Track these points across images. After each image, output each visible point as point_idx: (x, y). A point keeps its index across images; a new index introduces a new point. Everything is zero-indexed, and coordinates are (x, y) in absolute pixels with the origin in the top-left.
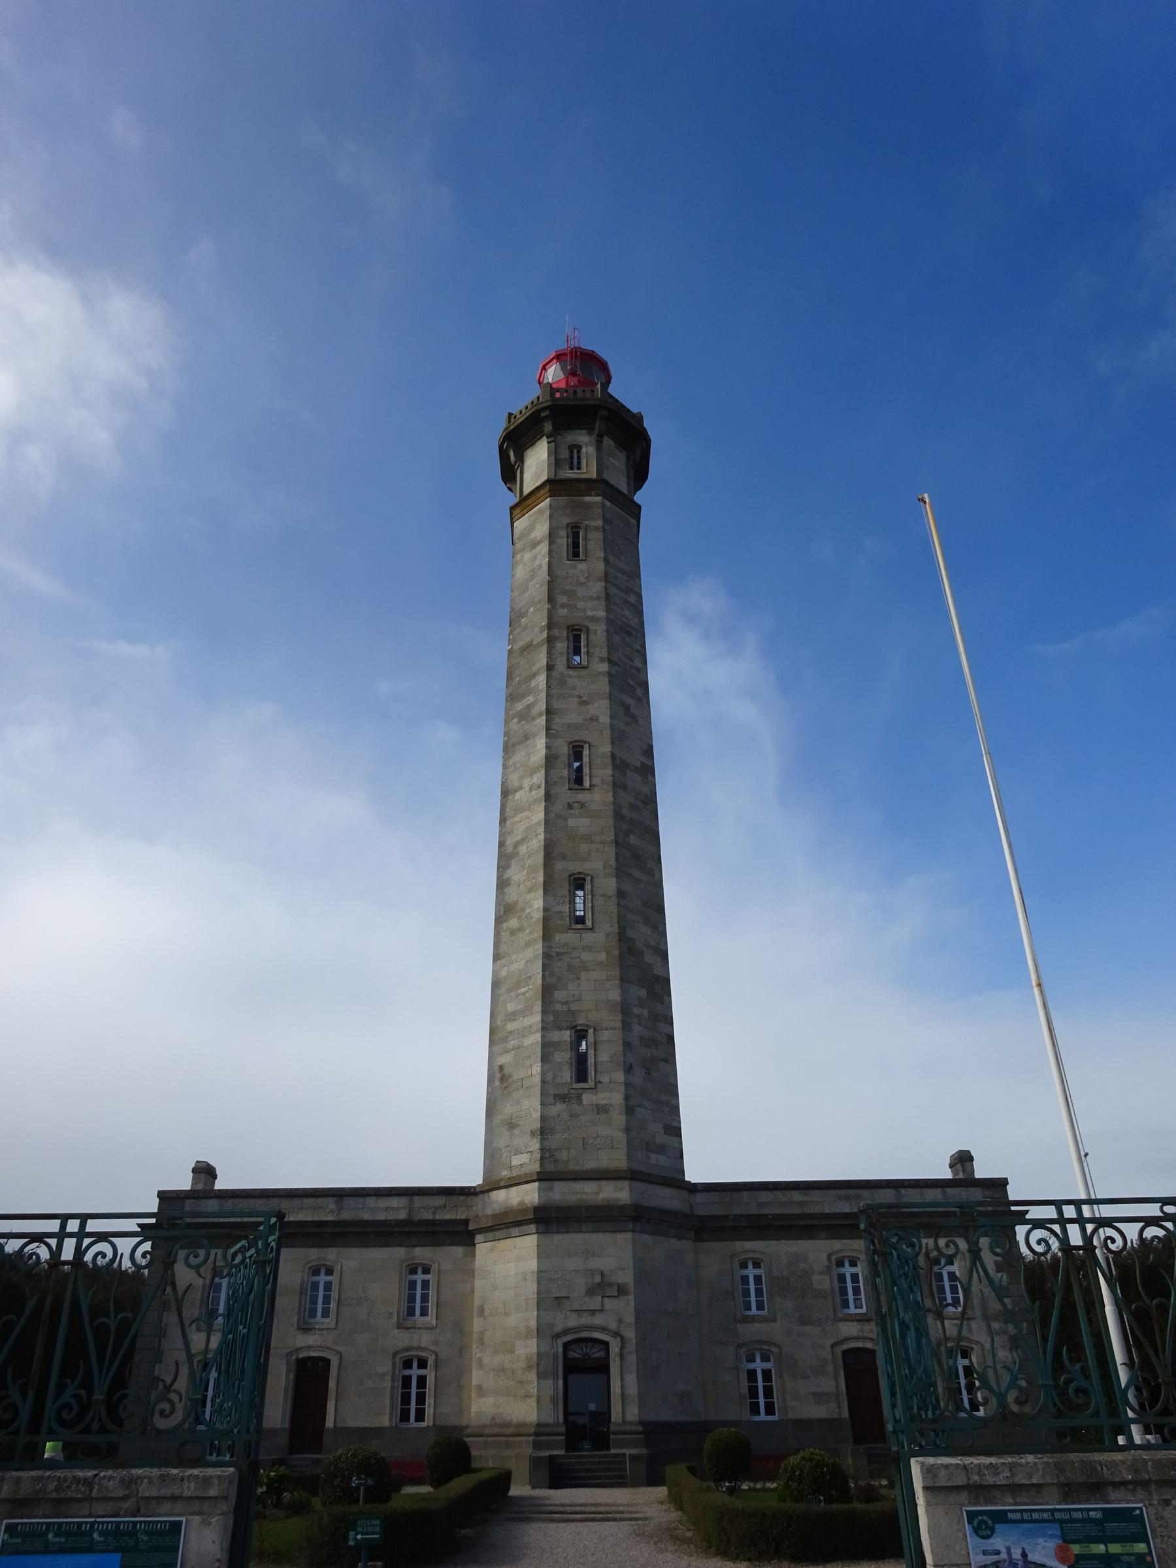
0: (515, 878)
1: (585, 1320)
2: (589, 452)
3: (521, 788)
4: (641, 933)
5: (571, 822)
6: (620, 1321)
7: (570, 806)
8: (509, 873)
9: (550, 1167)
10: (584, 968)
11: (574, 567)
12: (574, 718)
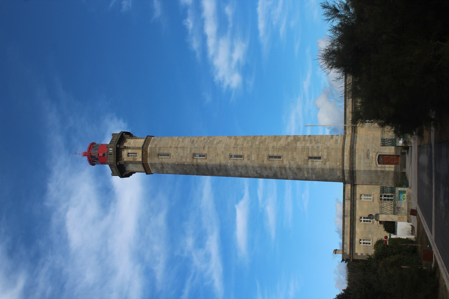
0: (267, 174)
1: (374, 159)
2: (130, 151)
3: (241, 172)
4: (282, 142)
5: (253, 159)
6: (375, 152)
7: (249, 159)
8: (265, 175)
9: (341, 167)
10: (293, 157)
11: (173, 156)
12: (222, 158)
